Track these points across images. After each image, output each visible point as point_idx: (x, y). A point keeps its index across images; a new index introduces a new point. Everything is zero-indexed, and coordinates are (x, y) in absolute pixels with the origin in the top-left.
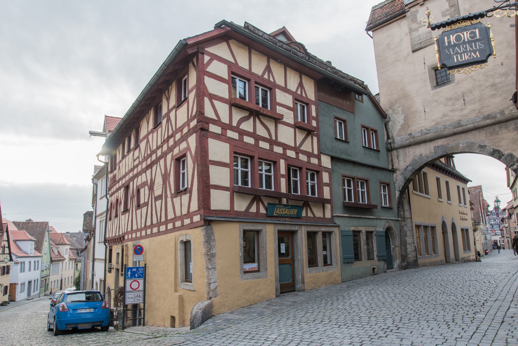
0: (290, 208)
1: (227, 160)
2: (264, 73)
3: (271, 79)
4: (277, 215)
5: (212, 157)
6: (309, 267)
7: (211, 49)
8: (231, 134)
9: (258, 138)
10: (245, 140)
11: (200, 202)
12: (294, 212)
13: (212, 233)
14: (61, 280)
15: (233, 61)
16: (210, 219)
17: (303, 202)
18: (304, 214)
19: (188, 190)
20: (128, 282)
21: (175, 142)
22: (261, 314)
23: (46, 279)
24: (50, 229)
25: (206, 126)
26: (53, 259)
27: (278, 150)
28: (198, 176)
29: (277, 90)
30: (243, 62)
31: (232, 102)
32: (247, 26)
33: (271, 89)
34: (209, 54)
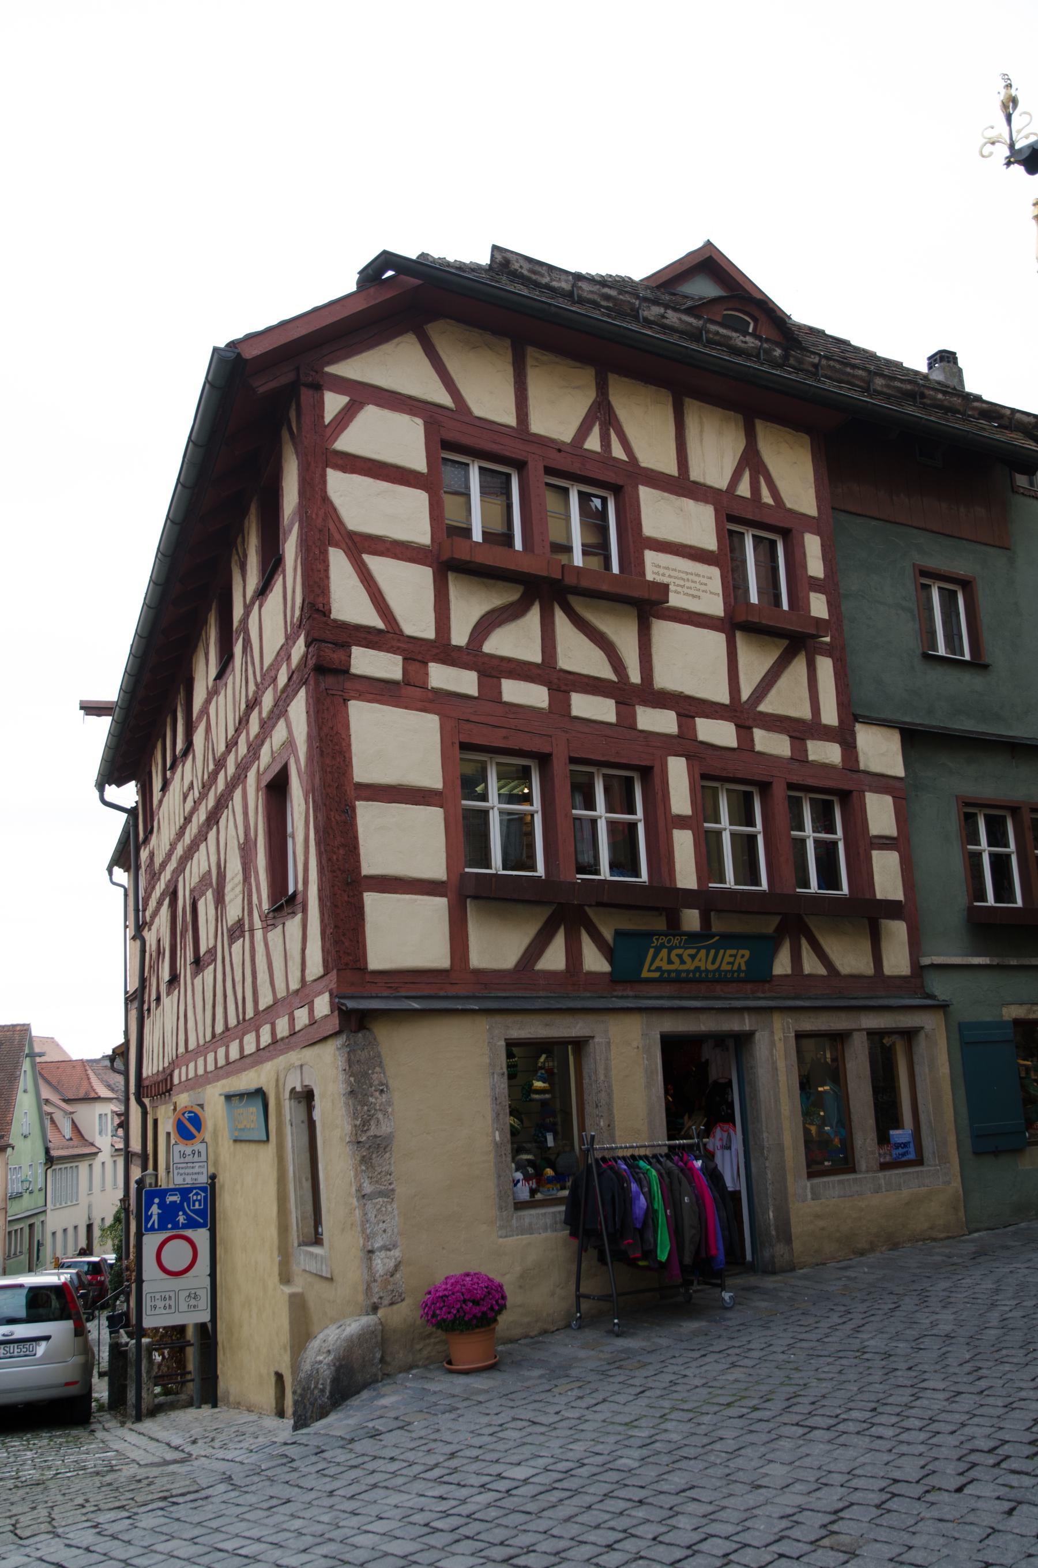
0: (717, 947)
1: (432, 778)
2: (583, 431)
3: (618, 452)
4: (657, 975)
5: (365, 770)
6: (811, 1175)
7: (352, 368)
8: (441, 676)
9: (563, 684)
10: (507, 697)
11: (328, 944)
12: (735, 959)
13: (377, 1061)
14: (90, 1227)
15: (445, 399)
16: (366, 1005)
17: (775, 921)
18: (782, 965)
19: (299, 898)
20: (151, 1242)
21: (263, 724)
22: (560, 1371)
23: (31, 1226)
24: (37, 1050)
25: (335, 657)
26: (54, 1153)
27: (656, 721)
28: (318, 844)
29: (645, 493)
30: (490, 398)
31: (445, 557)
32: (504, 261)
33: (617, 490)
34: (342, 385)
